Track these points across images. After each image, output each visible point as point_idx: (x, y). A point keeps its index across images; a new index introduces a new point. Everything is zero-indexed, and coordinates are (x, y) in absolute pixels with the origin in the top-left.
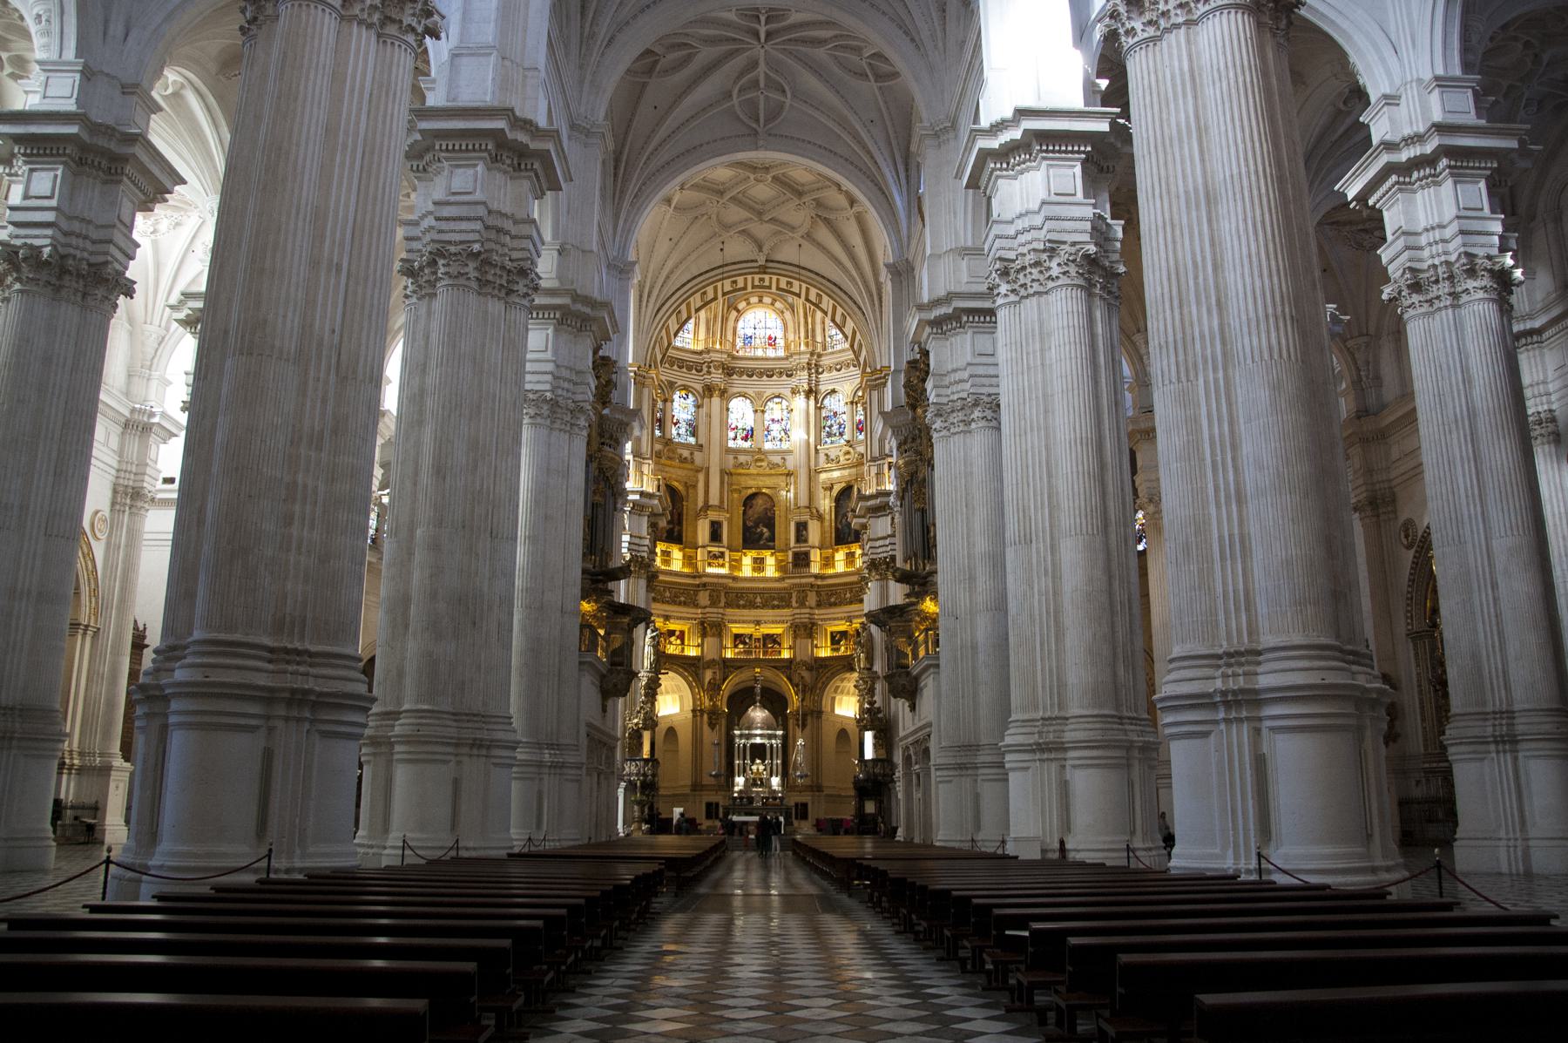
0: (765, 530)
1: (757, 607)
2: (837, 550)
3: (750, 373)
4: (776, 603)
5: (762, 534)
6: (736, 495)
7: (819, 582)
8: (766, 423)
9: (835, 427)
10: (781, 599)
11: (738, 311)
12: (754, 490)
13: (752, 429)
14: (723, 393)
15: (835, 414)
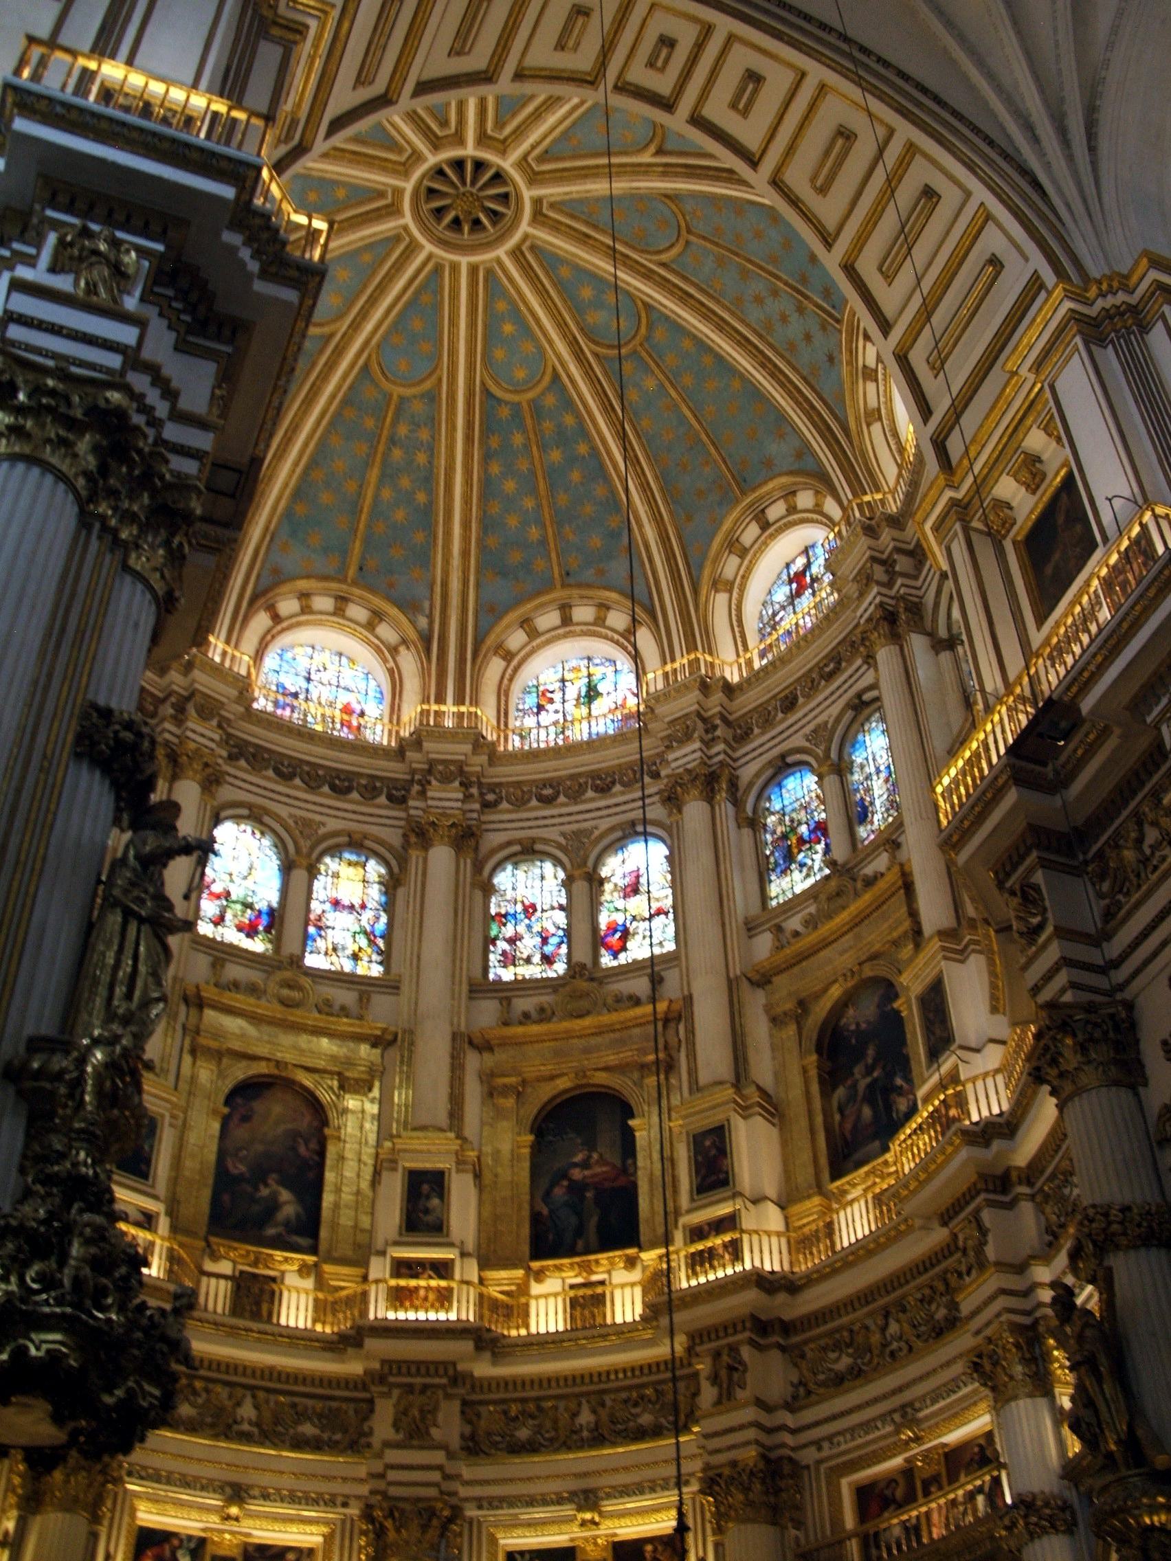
0: (285, 1195)
1: (246, 1438)
2: (539, 1276)
3: (287, 769)
4: (308, 1429)
5: (273, 1206)
6: (205, 1073)
7: (484, 1369)
8: (316, 907)
9: (529, 945)
10: (329, 1419)
11: (276, 618)
12: (262, 1068)
13: (271, 912)
14: (211, 782)
15: (530, 910)
